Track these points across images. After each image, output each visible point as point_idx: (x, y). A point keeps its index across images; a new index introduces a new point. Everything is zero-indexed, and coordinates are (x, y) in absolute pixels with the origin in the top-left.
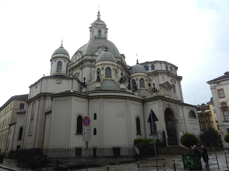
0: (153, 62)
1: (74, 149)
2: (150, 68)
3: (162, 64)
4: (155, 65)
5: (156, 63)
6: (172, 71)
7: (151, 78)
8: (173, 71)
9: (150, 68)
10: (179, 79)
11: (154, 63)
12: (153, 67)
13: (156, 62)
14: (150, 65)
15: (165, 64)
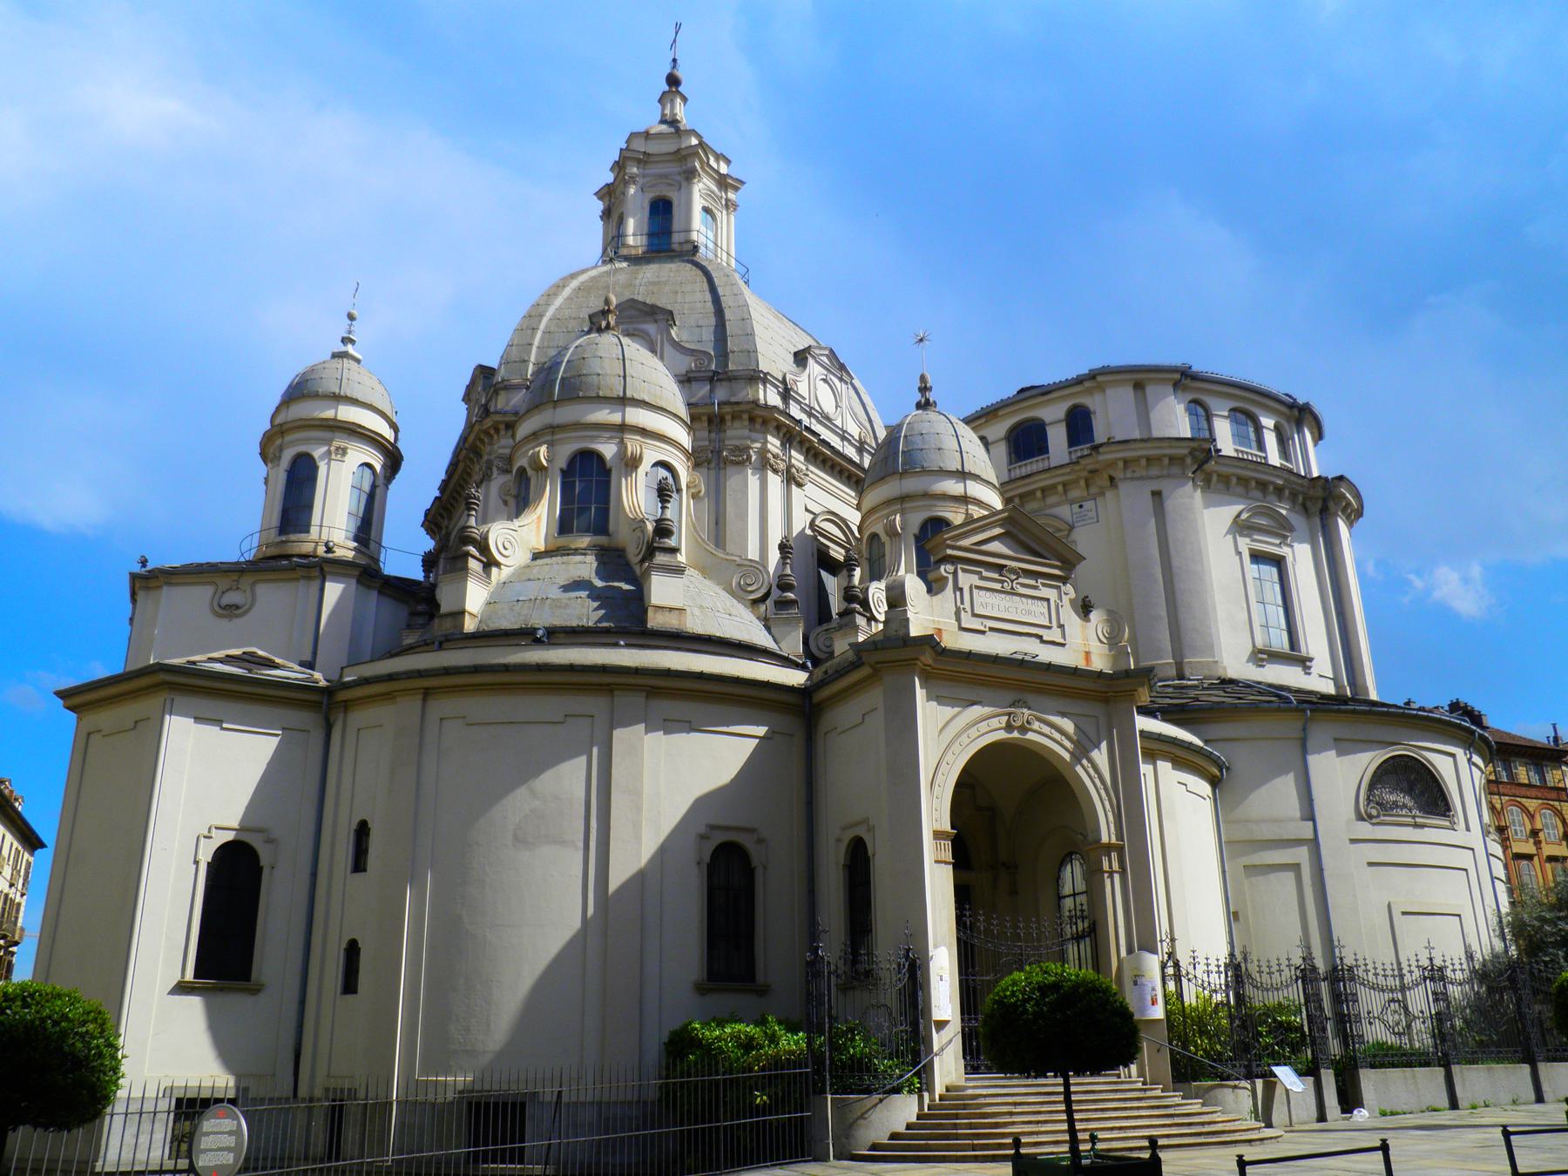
0: (1079, 381)
1: (163, 1105)
2: (1057, 437)
3: (1151, 390)
4: (1092, 402)
5: (1101, 388)
6: (1261, 446)
7: (1068, 517)
8: (1270, 440)
9: (1057, 437)
10: (1325, 500)
11: (1089, 392)
12: (1079, 424)
13: (1095, 379)
14: (1053, 413)
15: (1176, 385)
